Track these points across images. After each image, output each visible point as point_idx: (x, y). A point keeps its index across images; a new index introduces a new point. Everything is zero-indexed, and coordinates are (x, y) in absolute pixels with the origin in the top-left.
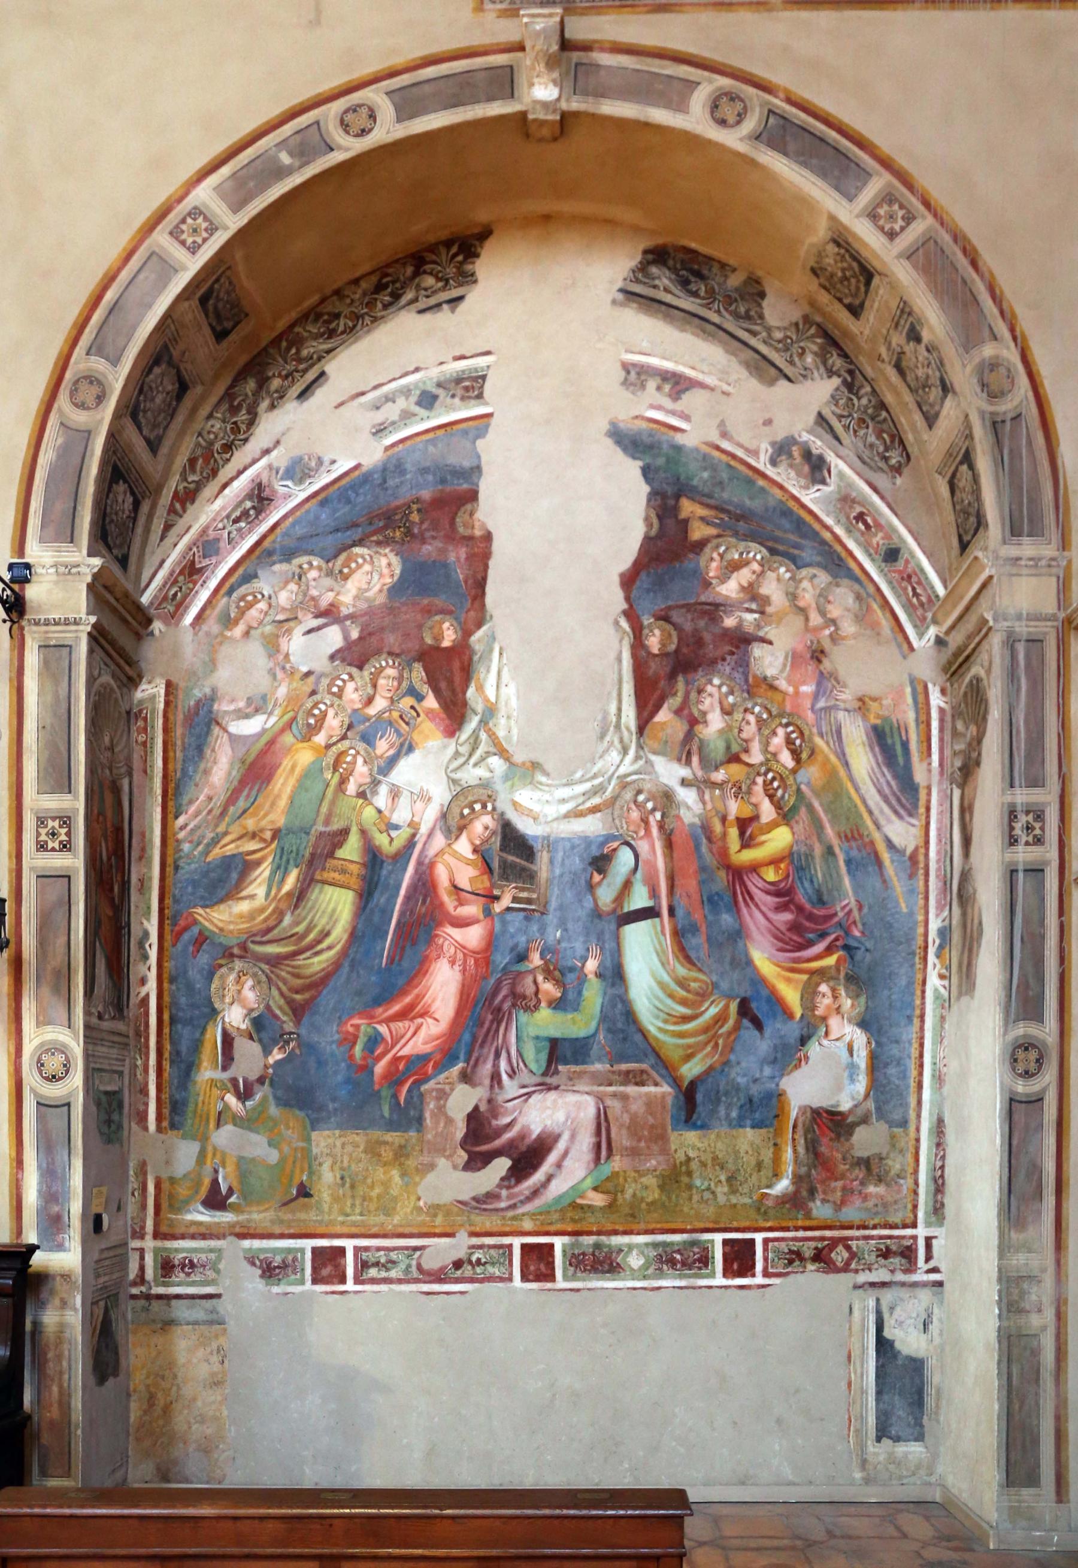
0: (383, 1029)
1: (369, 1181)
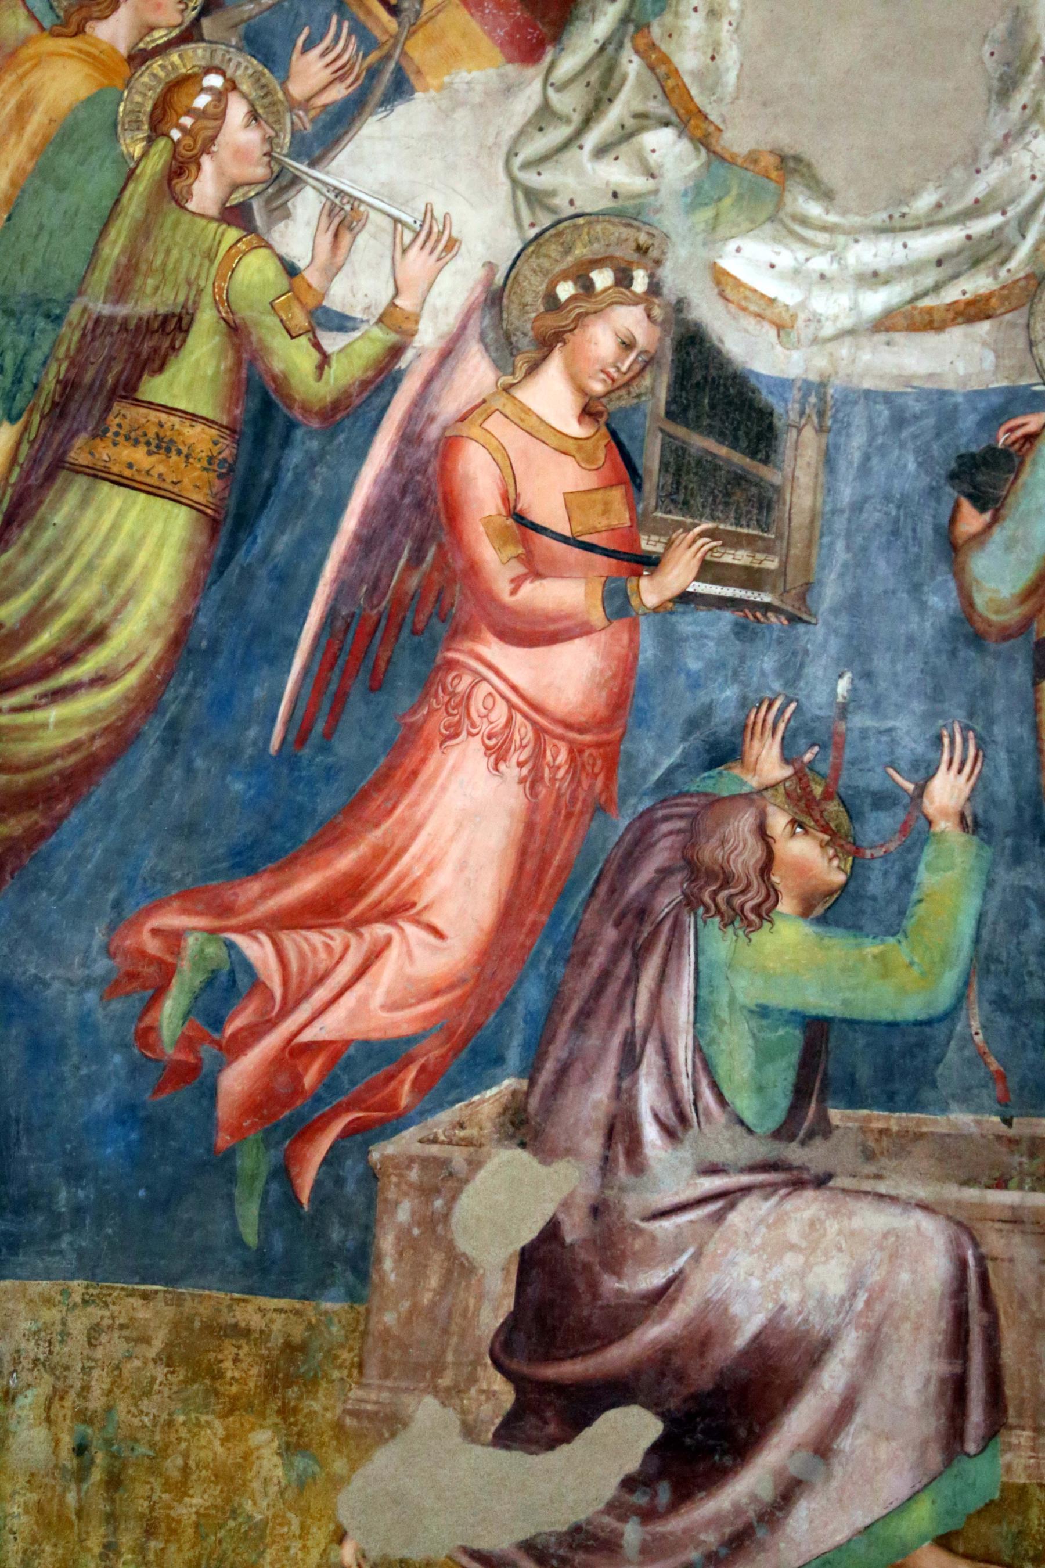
0: (258, 950)
1: (173, 1465)
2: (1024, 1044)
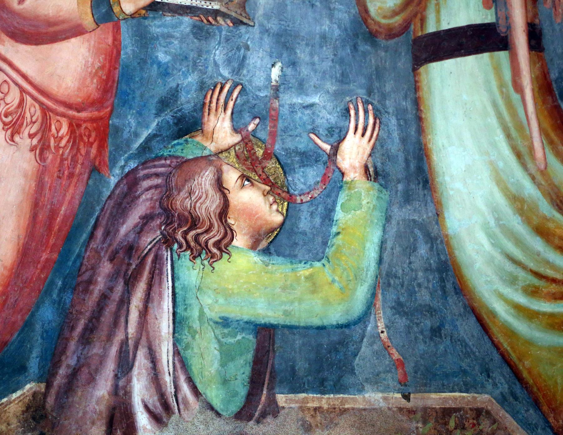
2: (416, 338)
